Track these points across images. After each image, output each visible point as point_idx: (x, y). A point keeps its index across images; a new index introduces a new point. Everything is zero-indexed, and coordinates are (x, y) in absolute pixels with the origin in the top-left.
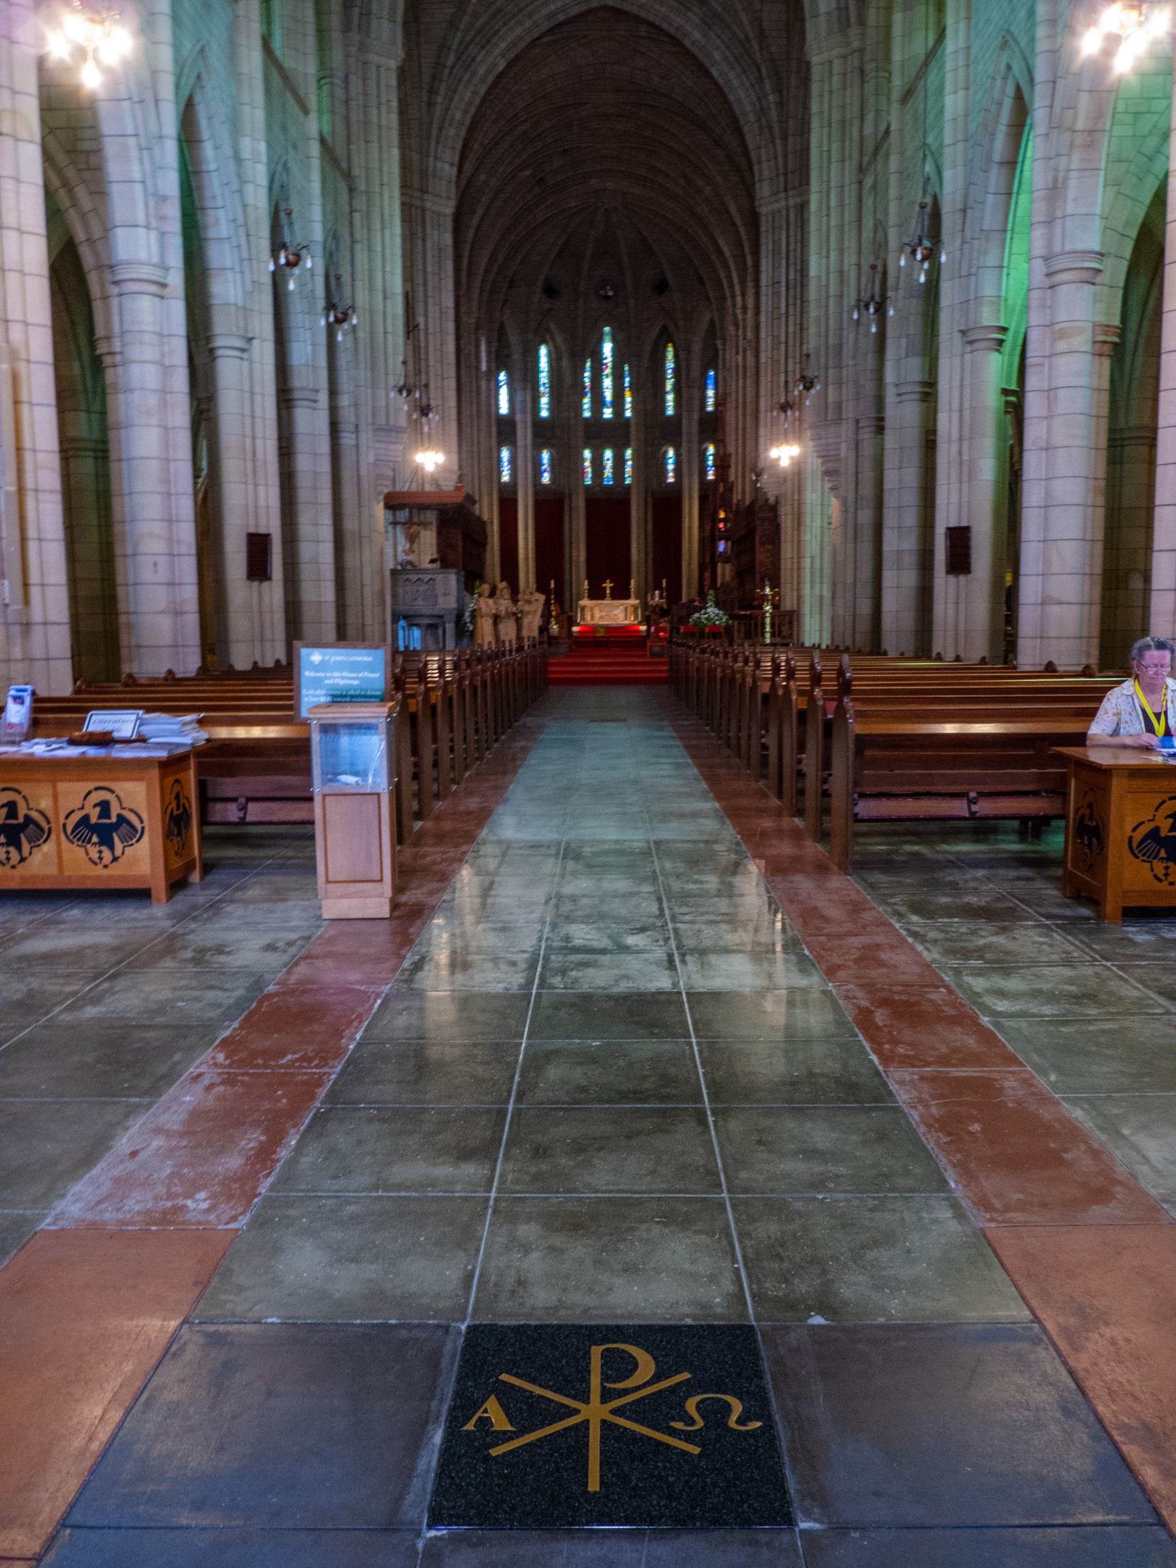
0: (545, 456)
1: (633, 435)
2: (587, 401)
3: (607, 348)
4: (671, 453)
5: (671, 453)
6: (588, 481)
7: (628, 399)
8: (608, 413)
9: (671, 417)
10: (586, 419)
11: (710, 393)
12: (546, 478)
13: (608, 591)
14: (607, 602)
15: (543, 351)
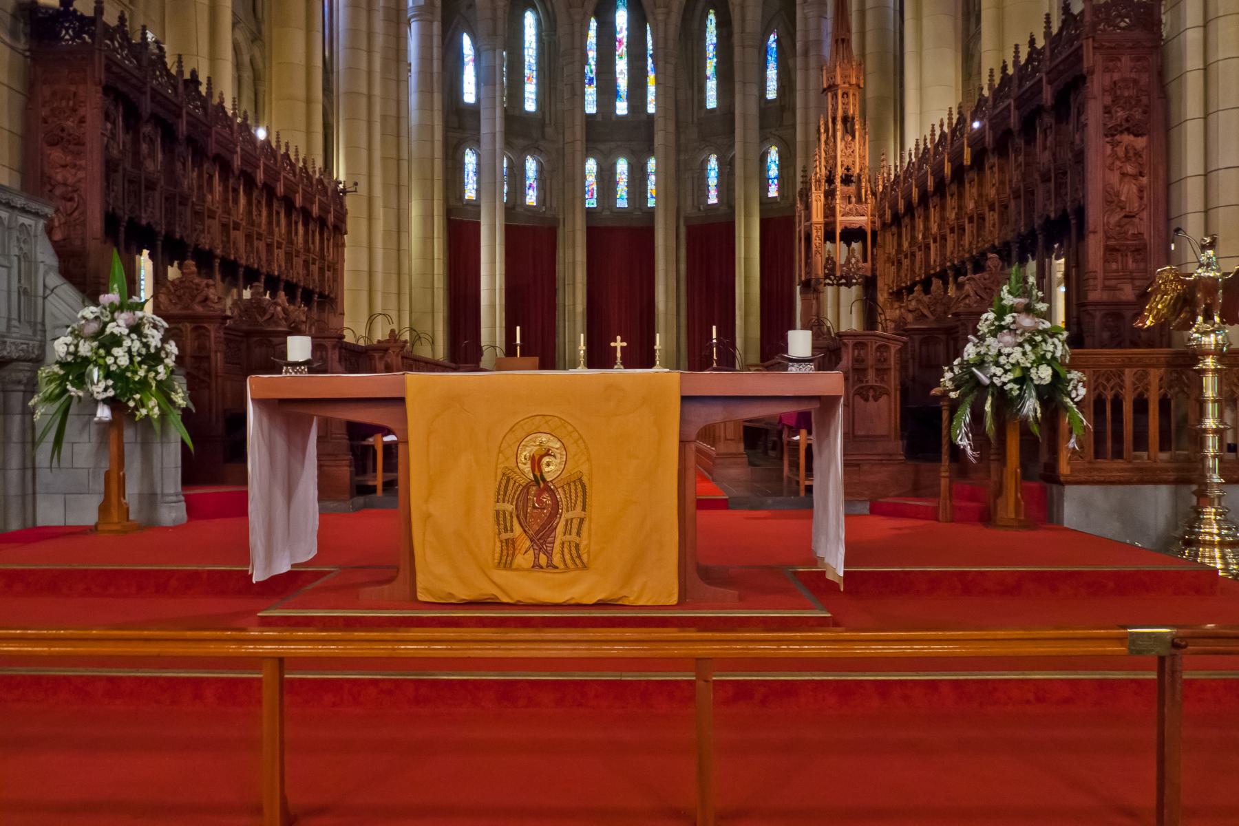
0: (531, 166)
1: (659, 139)
2: (591, 92)
3: (621, 18)
4: (713, 163)
5: (713, 163)
6: (591, 203)
7: (651, 89)
8: (622, 108)
9: (712, 110)
10: (591, 115)
11: (772, 73)
12: (531, 198)
13: (619, 355)
14: (618, 371)
15: (530, 19)
